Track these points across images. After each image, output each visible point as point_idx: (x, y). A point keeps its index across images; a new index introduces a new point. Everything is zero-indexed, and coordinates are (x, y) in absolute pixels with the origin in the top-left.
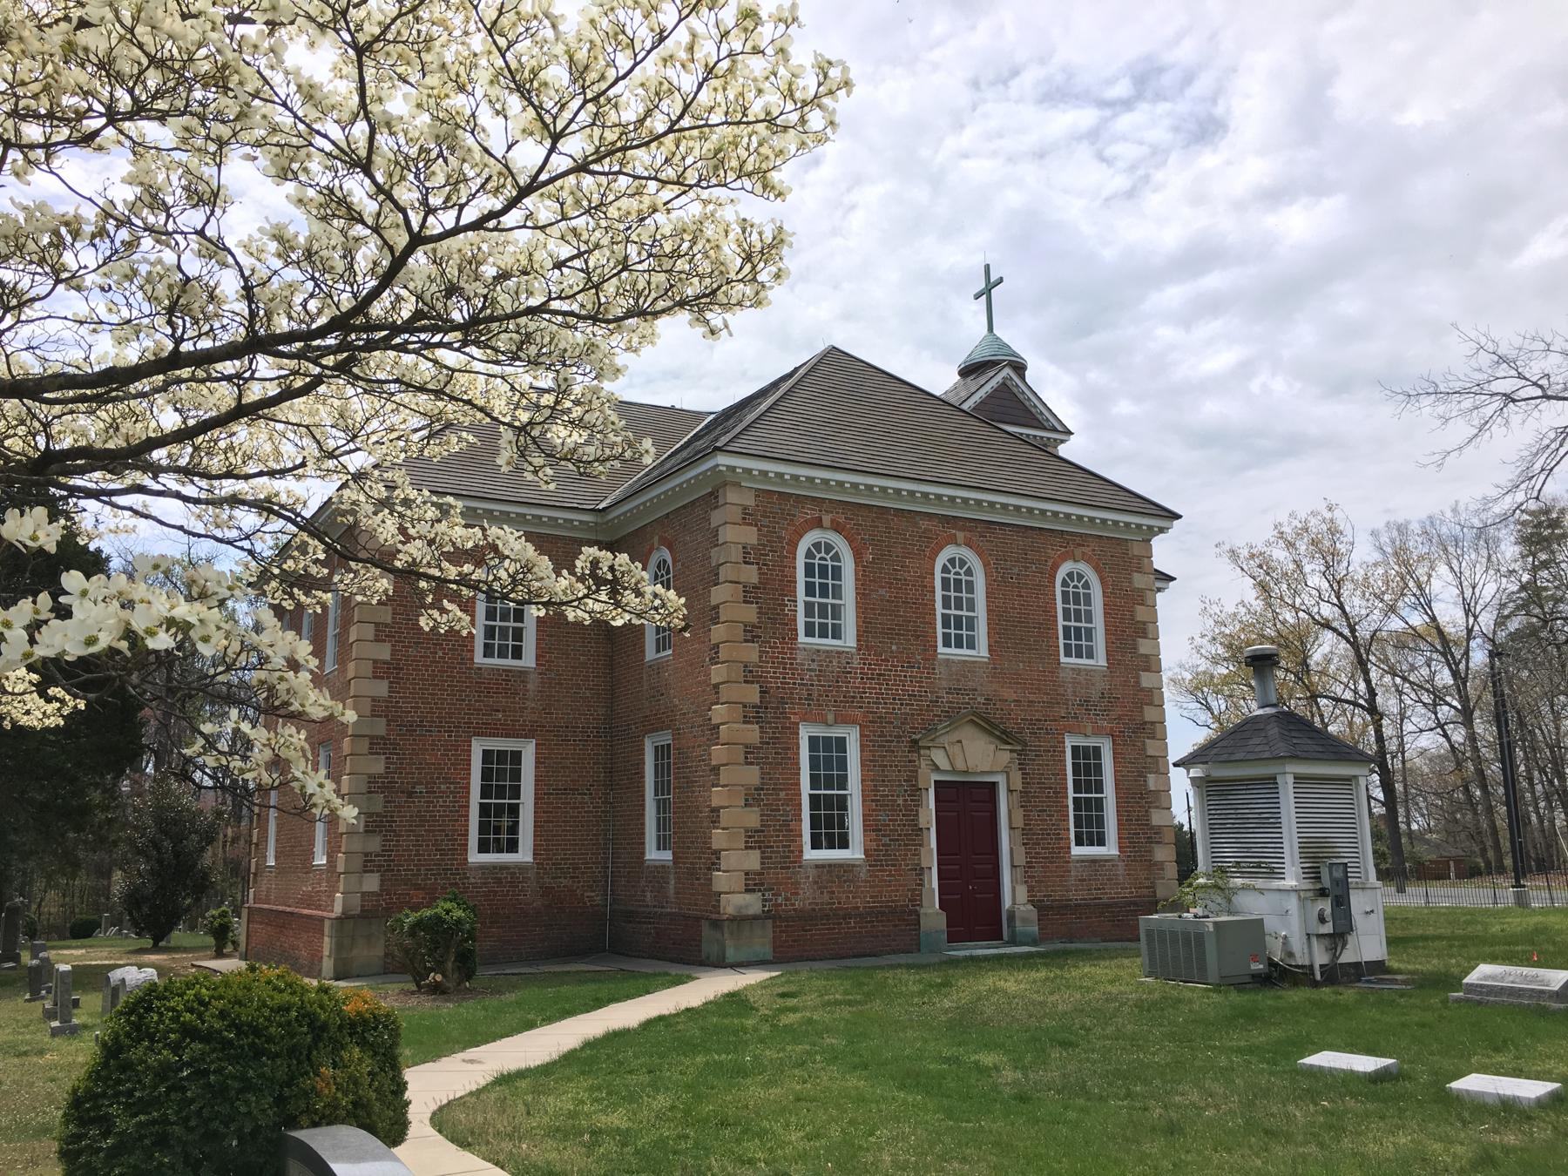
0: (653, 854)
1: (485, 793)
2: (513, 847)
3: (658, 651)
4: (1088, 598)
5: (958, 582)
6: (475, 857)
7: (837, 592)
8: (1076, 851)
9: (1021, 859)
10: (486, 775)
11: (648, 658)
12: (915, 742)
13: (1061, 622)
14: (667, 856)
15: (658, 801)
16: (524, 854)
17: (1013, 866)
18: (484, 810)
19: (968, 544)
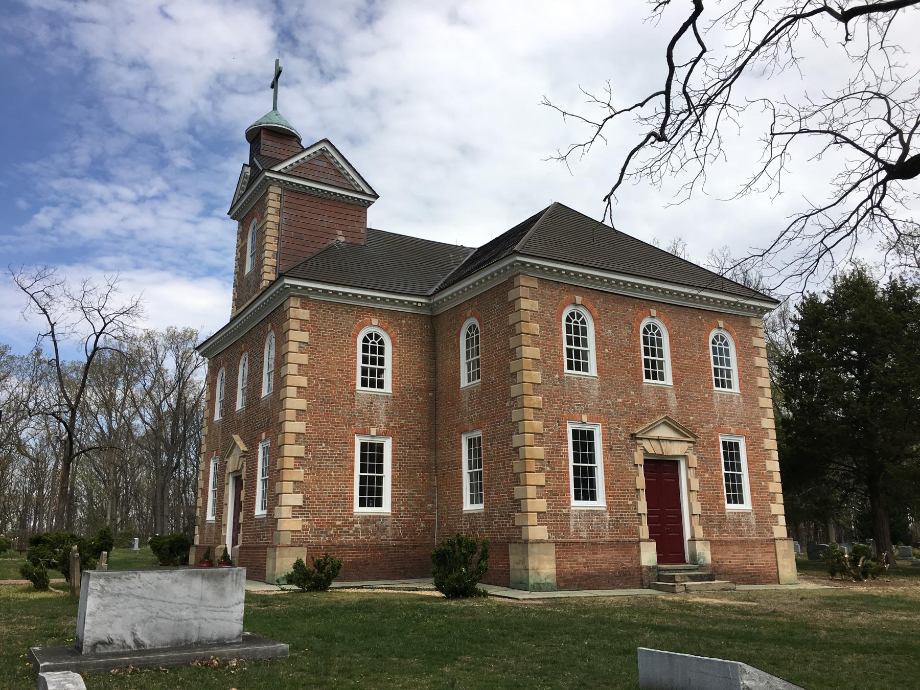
0: (468, 506)
1: (363, 469)
2: (379, 504)
3: (469, 381)
4: (727, 351)
5: (652, 340)
6: (358, 509)
7: (585, 344)
8: (729, 507)
9: (697, 510)
10: (363, 457)
11: (462, 386)
12: (633, 437)
13: (713, 366)
14: (481, 506)
15: (471, 474)
16: (386, 508)
17: (692, 515)
18: (363, 480)
19: (659, 316)
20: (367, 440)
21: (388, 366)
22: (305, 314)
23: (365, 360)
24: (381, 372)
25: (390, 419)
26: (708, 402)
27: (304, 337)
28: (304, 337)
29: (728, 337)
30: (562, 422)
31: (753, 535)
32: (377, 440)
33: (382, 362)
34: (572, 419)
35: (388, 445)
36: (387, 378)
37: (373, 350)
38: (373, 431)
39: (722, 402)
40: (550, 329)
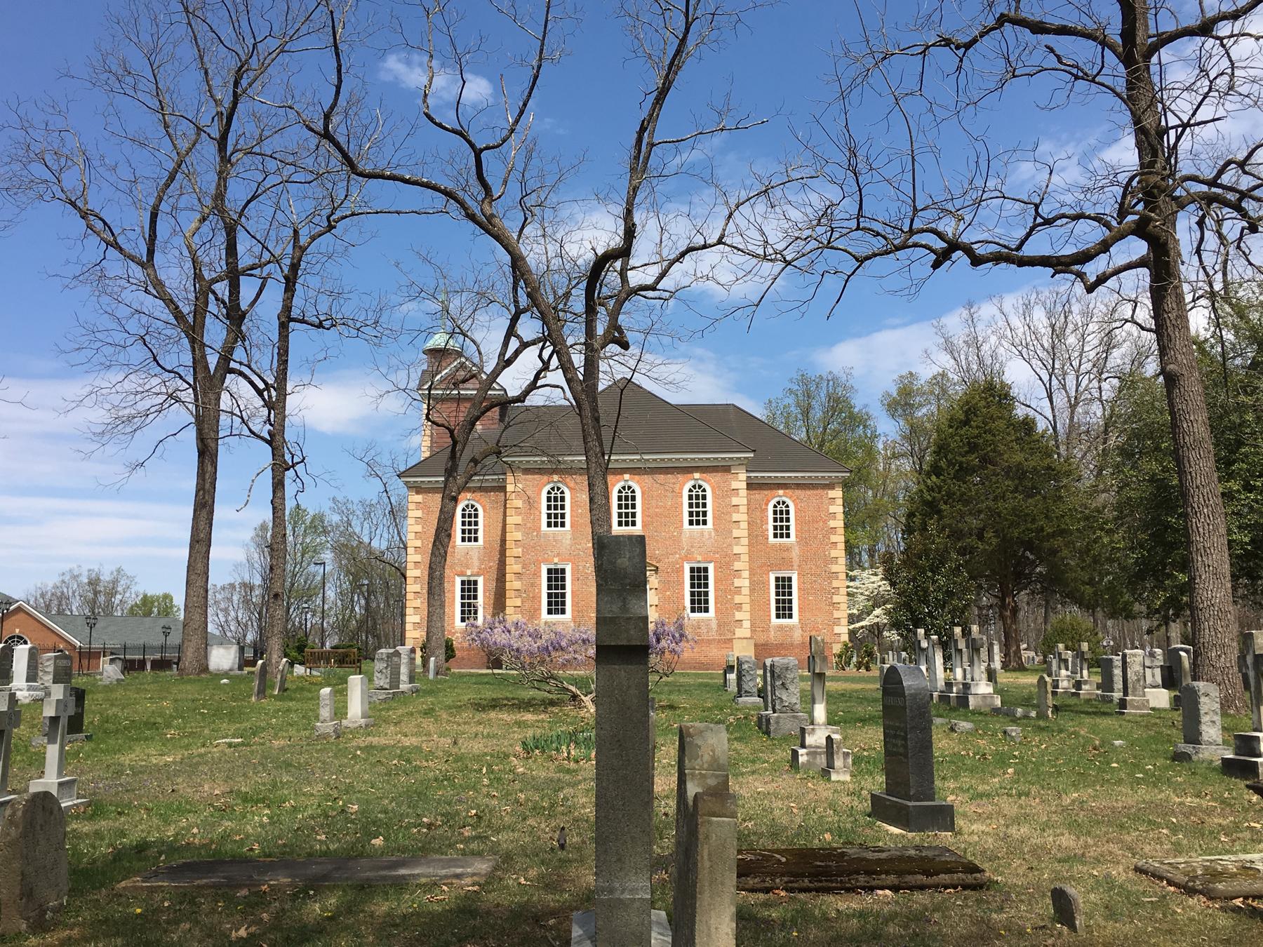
19: (632, 479)
20: (465, 578)
21: (481, 527)
22: (419, 498)
23: (463, 523)
24: (476, 531)
25: (481, 561)
26: (677, 540)
27: (419, 513)
28: (419, 513)
29: (705, 485)
30: (537, 564)
31: (714, 635)
32: (472, 579)
33: (476, 524)
34: (545, 561)
35: (480, 581)
36: (480, 535)
37: (470, 516)
38: (469, 573)
39: (691, 537)
40: (531, 503)
